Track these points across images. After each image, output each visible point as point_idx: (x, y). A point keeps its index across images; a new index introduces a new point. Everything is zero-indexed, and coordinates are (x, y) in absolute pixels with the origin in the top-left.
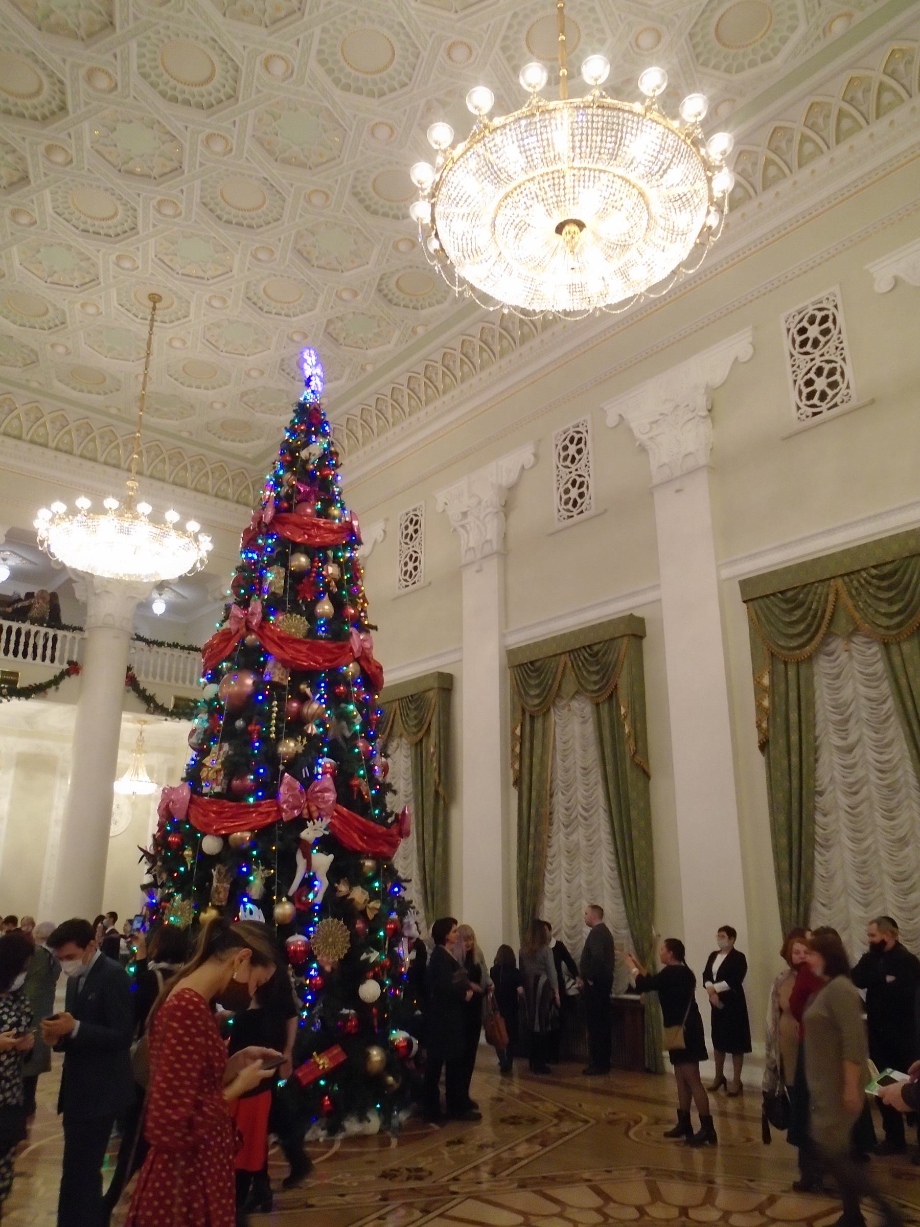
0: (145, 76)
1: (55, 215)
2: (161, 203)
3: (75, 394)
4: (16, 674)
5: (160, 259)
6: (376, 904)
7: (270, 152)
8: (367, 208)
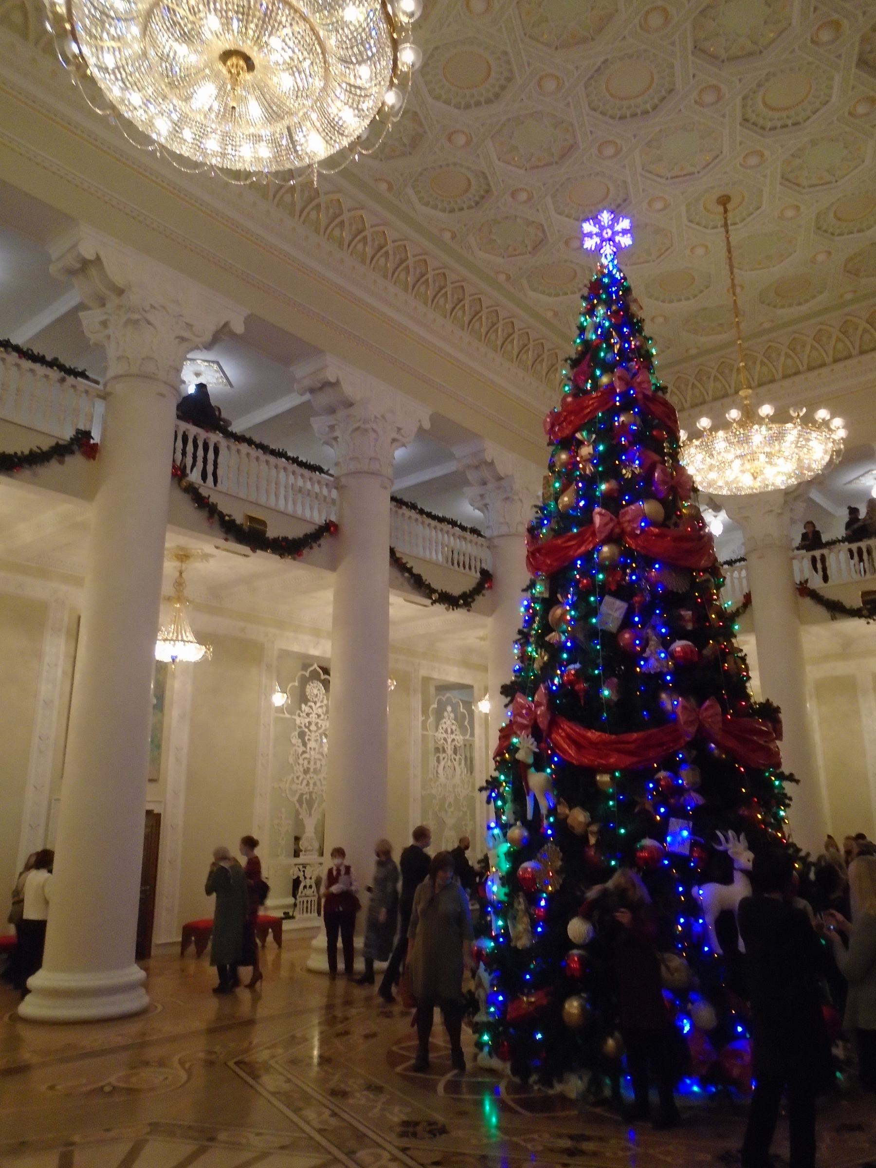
0: (468, 106)
3: (804, 308)
5: (672, 178)
6: (594, 828)
7: (584, 40)
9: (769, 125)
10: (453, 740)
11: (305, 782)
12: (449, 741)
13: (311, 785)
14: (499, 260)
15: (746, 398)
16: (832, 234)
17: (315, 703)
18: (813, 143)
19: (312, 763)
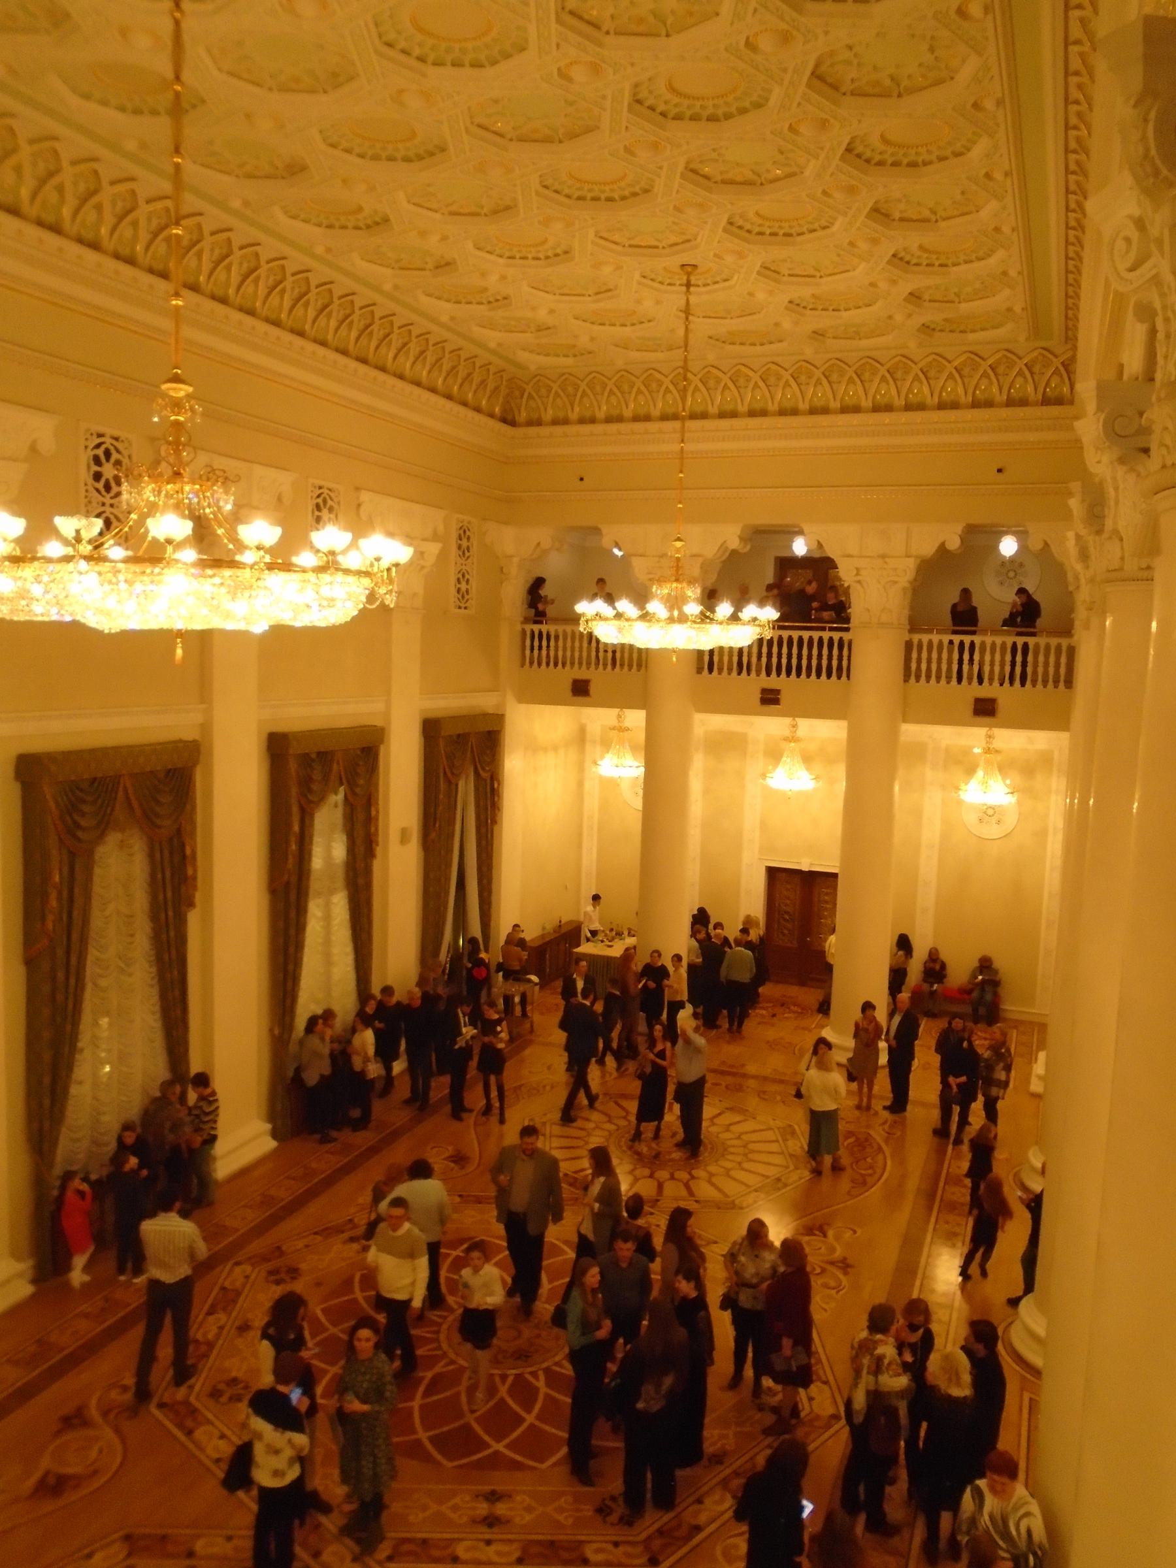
1: (511, 261)
4: (778, 692)
5: (630, 246)
7: (547, 140)
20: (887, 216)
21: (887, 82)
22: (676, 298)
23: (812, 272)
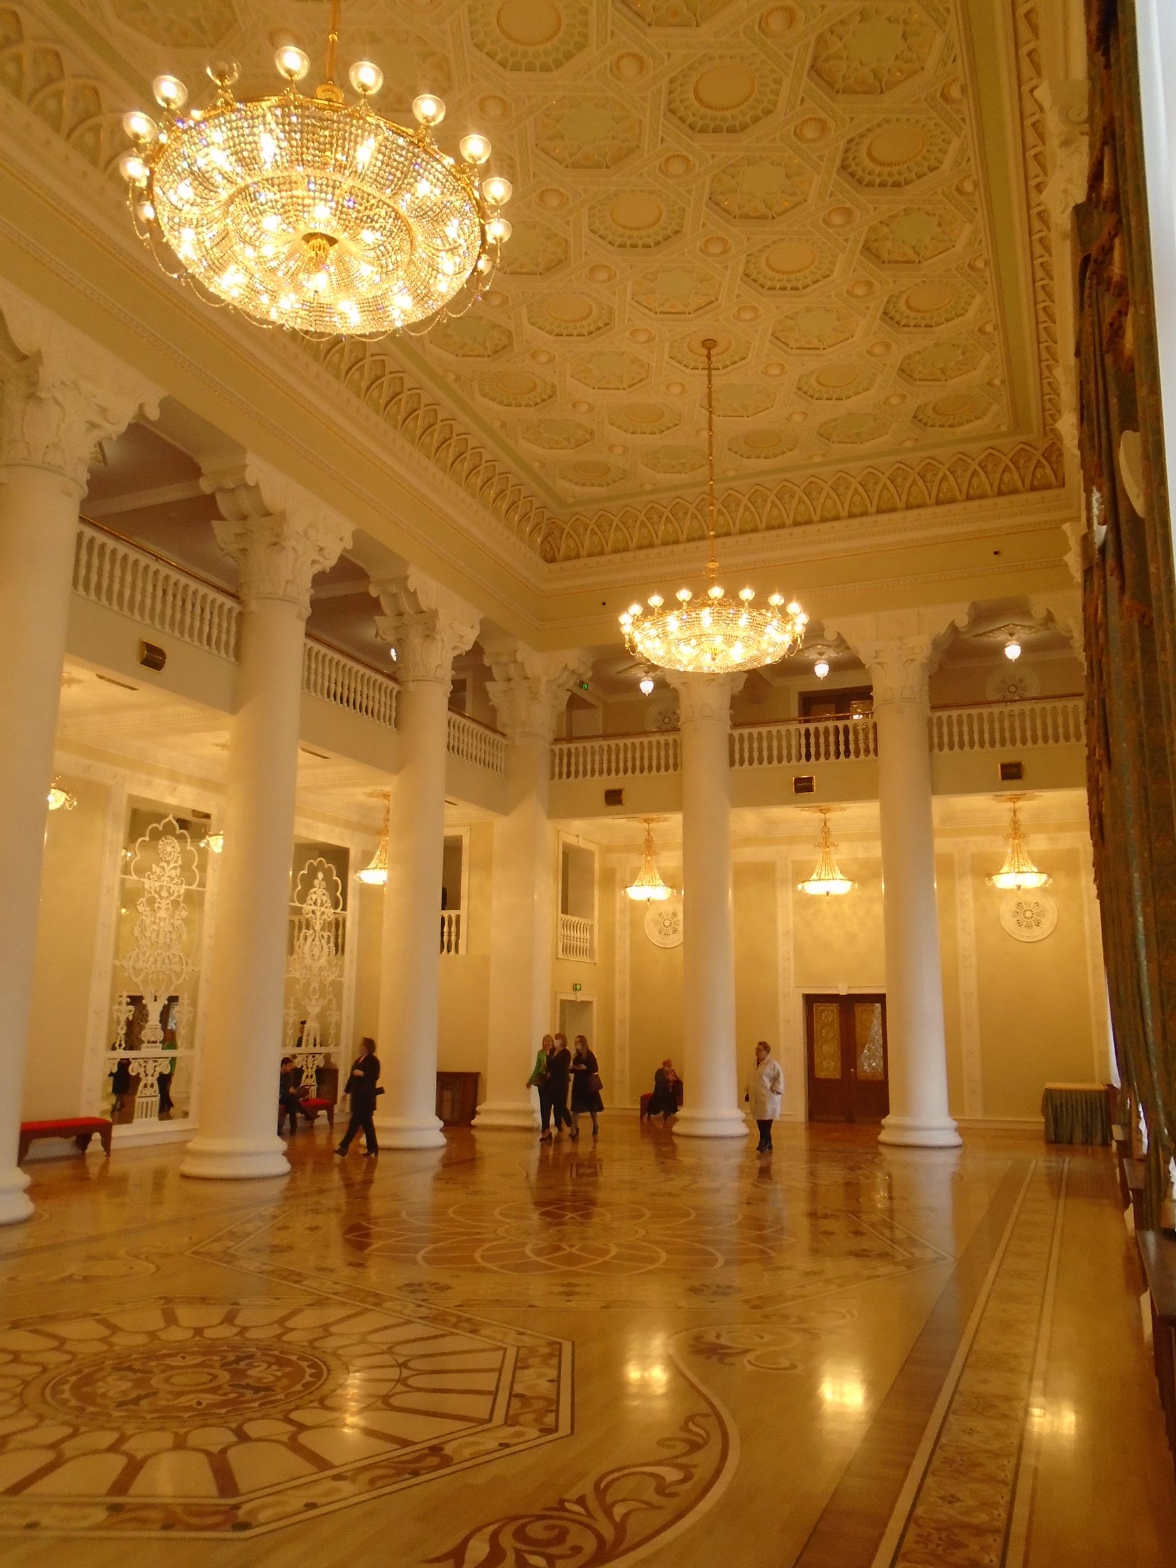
2: (592, 271)
4: (810, 779)
7: (598, 166)
8: (732, 130)
9: (768, 284)
10: (323, 913)
11: (152, 959)
12: (318, 914)
13: (159, 964)
14: (453, 358)
15: (713, 571)
16: (811, 397)
17: (168, 863)
18: (808, 310)
19: (161, 937)
20: (878, 258)
21: (871, 79)
22: (697, 382)
23: (816, 343)
